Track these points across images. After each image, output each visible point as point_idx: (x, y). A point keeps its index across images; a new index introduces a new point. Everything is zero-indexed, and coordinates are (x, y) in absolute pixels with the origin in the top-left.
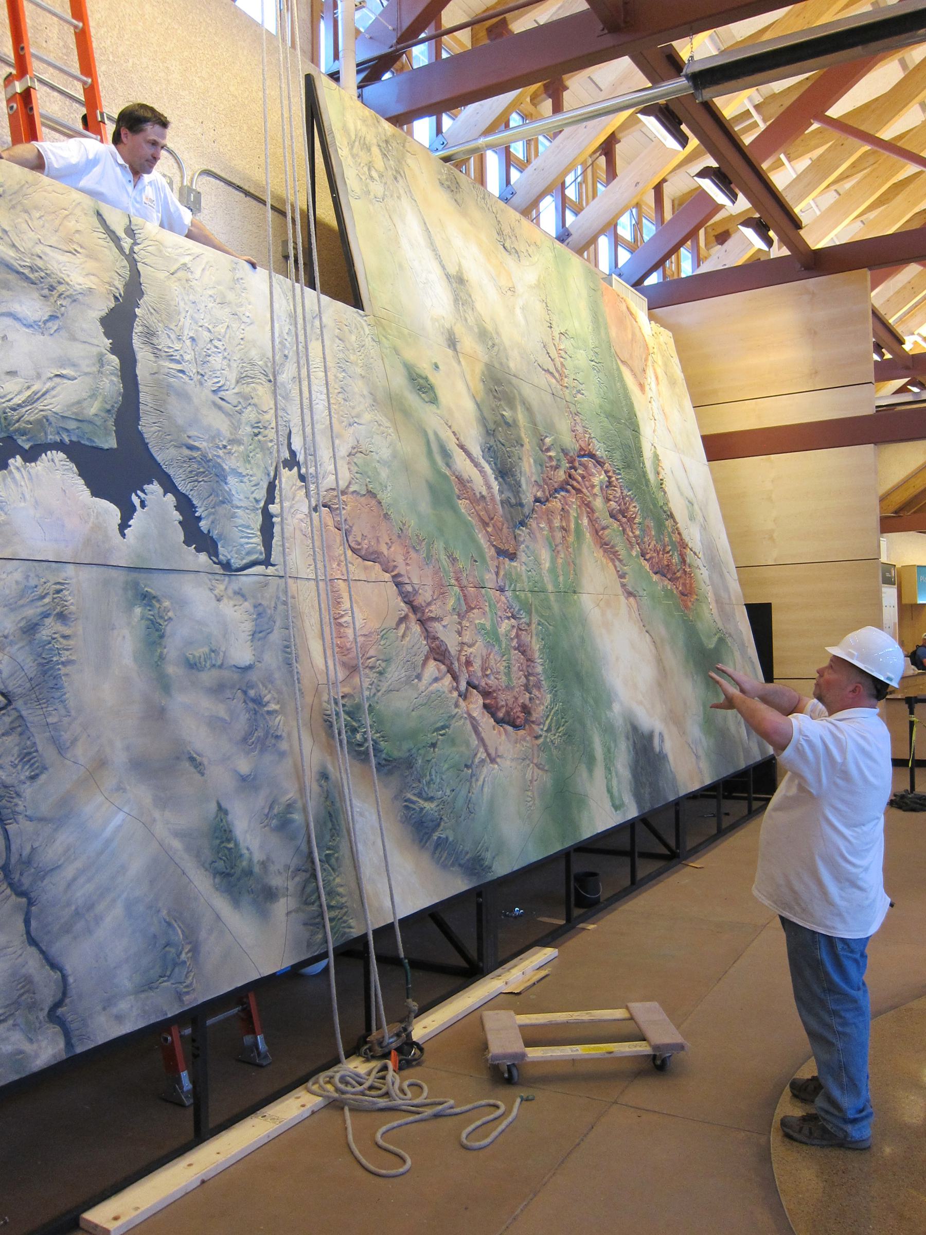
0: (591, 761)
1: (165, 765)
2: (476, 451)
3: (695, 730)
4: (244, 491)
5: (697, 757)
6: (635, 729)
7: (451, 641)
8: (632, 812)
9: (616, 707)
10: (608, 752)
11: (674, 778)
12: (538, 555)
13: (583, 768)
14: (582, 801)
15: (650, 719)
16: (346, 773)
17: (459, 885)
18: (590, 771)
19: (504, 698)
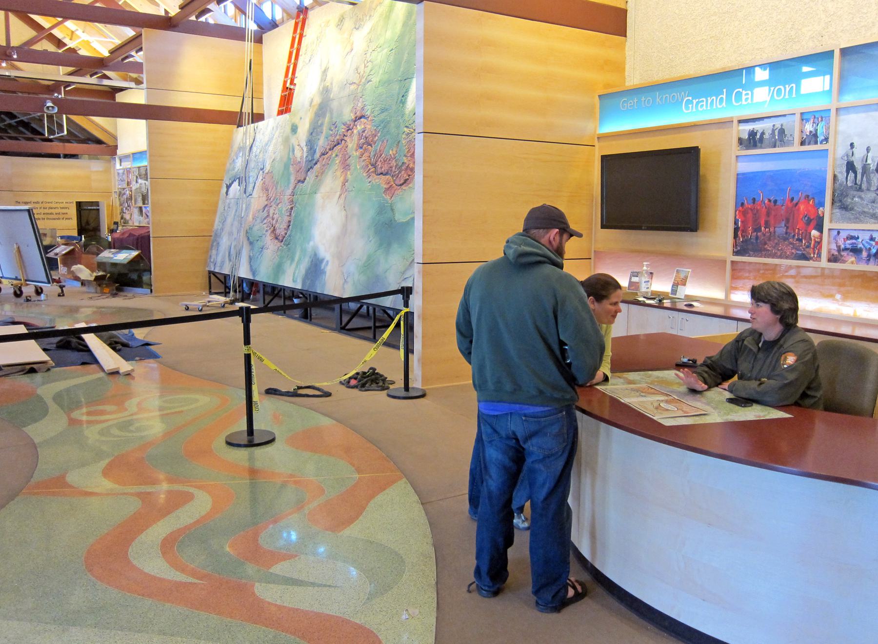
0: (293, 260)
1: (231, 234)
2: (303, 144)
3: (351, 267)
4: (251, 180)
5: (346, 281)
6: (315, 255)
7: (271, 212)
8: (299, 286)
9: (311, 243)
10: (300, 259)
11: (325, 284)
12: (311, 177)
13: (289, 262)
14: (284, 272)
15: (326, 252)
16: (246, 243)
17: (251, 277)
18: (291, 264)
19: (278, 232)
